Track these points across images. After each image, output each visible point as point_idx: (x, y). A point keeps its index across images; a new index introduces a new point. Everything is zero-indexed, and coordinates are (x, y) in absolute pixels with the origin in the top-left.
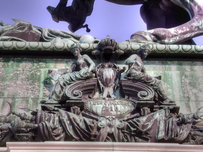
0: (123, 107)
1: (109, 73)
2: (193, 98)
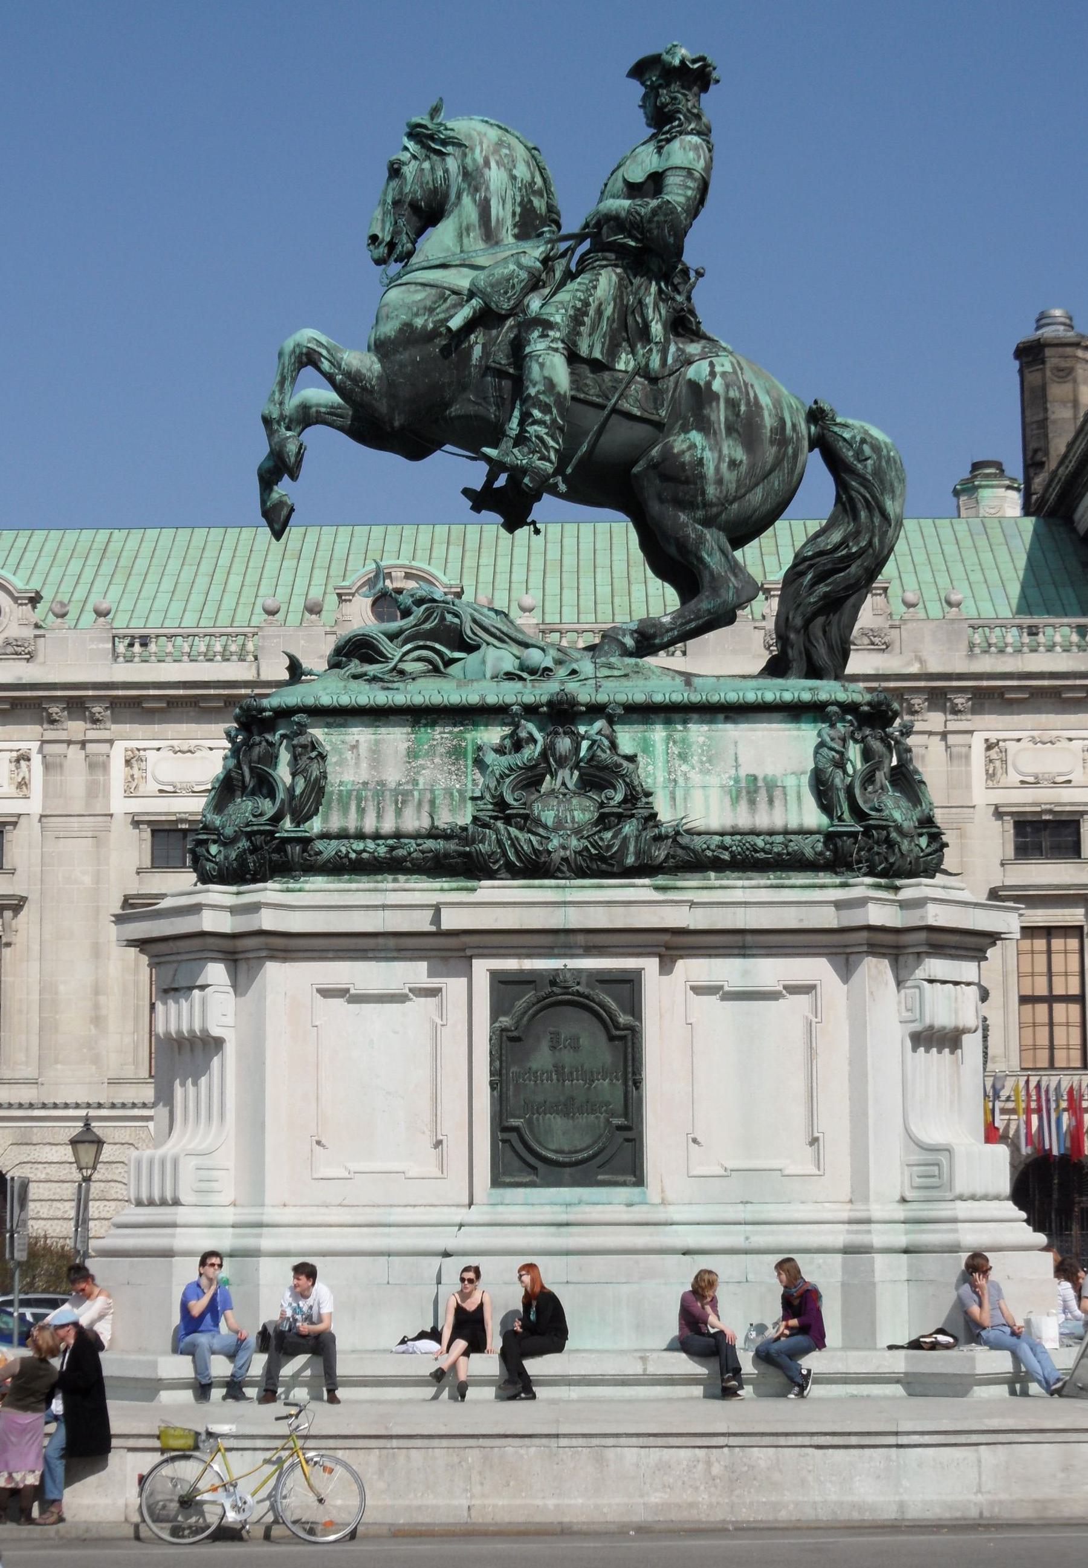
0: (582, 811)
1: (564, 744)
2: (681, 781)
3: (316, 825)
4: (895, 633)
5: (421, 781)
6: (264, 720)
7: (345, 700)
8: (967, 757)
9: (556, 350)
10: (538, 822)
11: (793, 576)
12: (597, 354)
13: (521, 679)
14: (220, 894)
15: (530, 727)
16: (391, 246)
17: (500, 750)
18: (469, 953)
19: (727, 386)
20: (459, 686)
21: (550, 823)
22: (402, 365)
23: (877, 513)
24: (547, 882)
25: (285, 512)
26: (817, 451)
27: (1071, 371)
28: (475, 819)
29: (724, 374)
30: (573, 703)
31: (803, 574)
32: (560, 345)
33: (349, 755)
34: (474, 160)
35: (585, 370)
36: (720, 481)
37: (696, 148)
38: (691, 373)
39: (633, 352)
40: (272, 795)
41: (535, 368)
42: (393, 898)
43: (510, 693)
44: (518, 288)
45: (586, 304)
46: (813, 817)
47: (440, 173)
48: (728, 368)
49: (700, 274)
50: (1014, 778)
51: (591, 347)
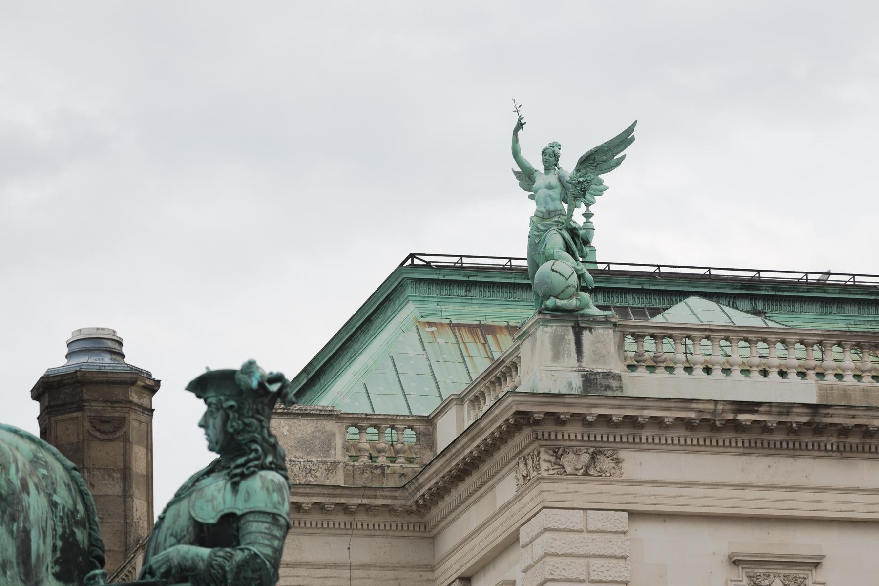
27: (121, 422)
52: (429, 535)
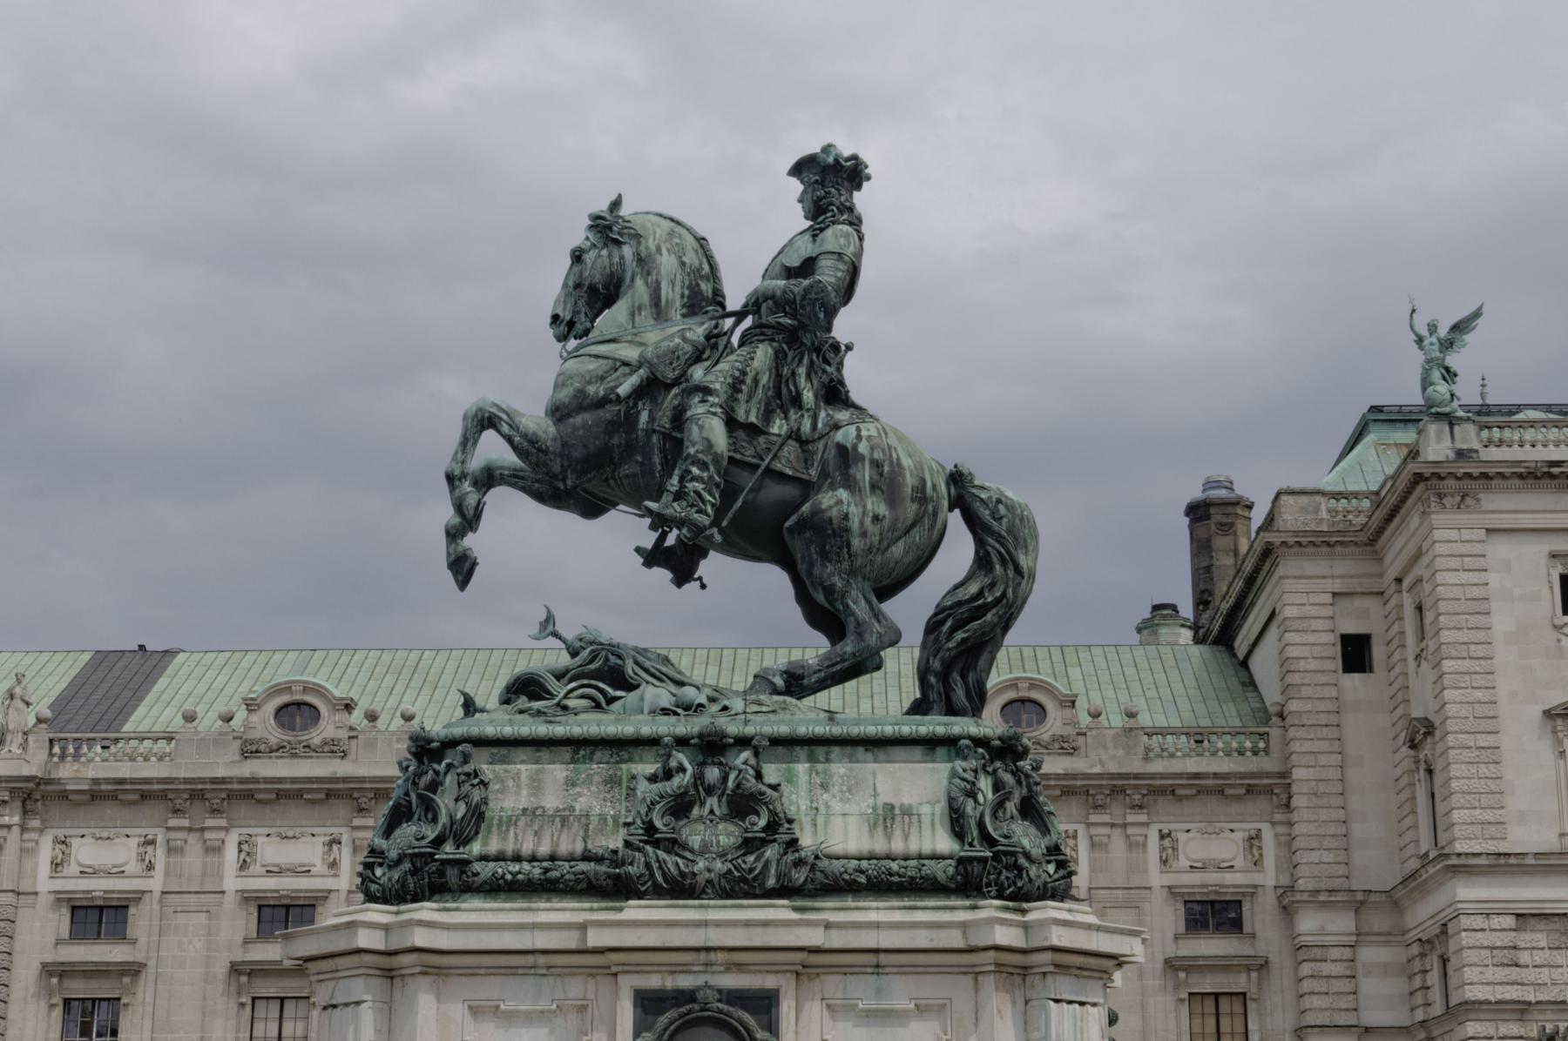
0: (727, 835)
1: (713, 774)
2: (822, 809)
3: (476, 848)
4: (1081, 739)
5: (578, 807)
6: (431, 751)
7: (508, 731)
8: (1144, 845)
9: (715, 414)
10: (685, 847)
11: (932, 627)
12: (753, 419)
13: (676, 714)
14: (379, 913)
15: (680, 757)
16: (571, 324)
17: (653, 779)
18: (614, 969)
19: (872, 449)
20: (617, 720)
21: (696, 847)
22: (575, 428)
23: (1011, 566)
24: (691, 902)
25: (467, 565)
26: (957, 512)
27: (1232, 525)
28: (627, 844)
29: (869, 438)
30: (724, 736)
31: (943, 622)
32: (719, 410)
33: (510, 783)
34: (647, 248)
35: (741, 434)
36: (864, 534)
37: (847, 236)
38: (839, 436)
39: (786, 418)
40: (435, 820)
41: (695, 429)
42: (543, 917)
43: (666, 727)
44: (683, 359)
45: (744, 373)
46: (944, 843)
47: (616, 259)
48: (873, 432)
49: (849, 348)
50: (1184, 862)
51: (748, 413)
52: (1378, 557)
